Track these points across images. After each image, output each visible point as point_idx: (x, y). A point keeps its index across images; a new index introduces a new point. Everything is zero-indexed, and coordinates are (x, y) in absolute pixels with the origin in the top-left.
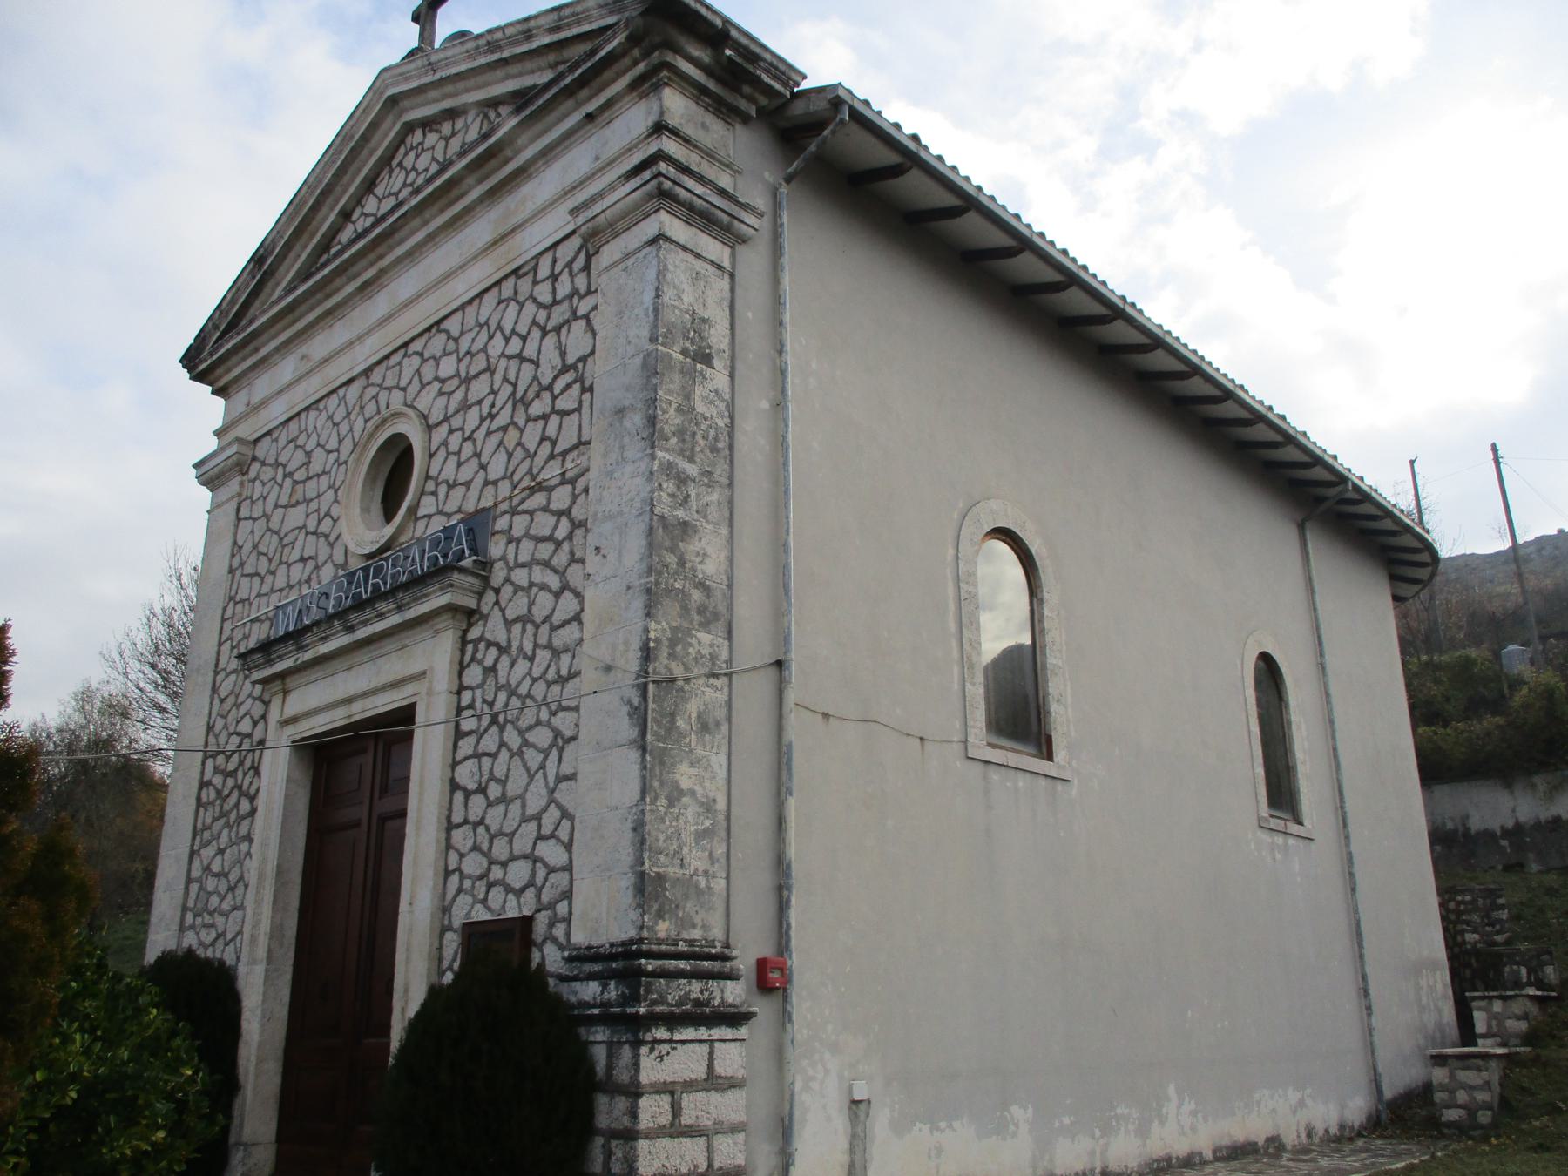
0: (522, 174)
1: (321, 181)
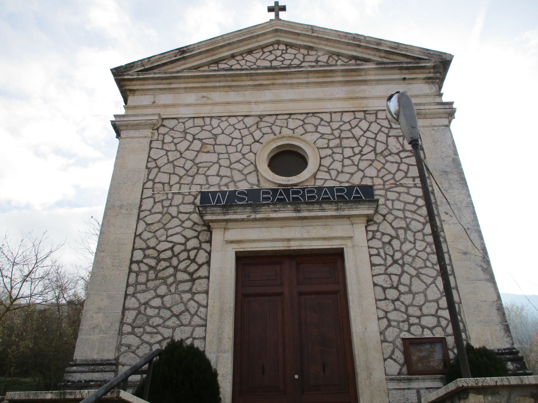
0: (365, 82)
1: (230, 39)
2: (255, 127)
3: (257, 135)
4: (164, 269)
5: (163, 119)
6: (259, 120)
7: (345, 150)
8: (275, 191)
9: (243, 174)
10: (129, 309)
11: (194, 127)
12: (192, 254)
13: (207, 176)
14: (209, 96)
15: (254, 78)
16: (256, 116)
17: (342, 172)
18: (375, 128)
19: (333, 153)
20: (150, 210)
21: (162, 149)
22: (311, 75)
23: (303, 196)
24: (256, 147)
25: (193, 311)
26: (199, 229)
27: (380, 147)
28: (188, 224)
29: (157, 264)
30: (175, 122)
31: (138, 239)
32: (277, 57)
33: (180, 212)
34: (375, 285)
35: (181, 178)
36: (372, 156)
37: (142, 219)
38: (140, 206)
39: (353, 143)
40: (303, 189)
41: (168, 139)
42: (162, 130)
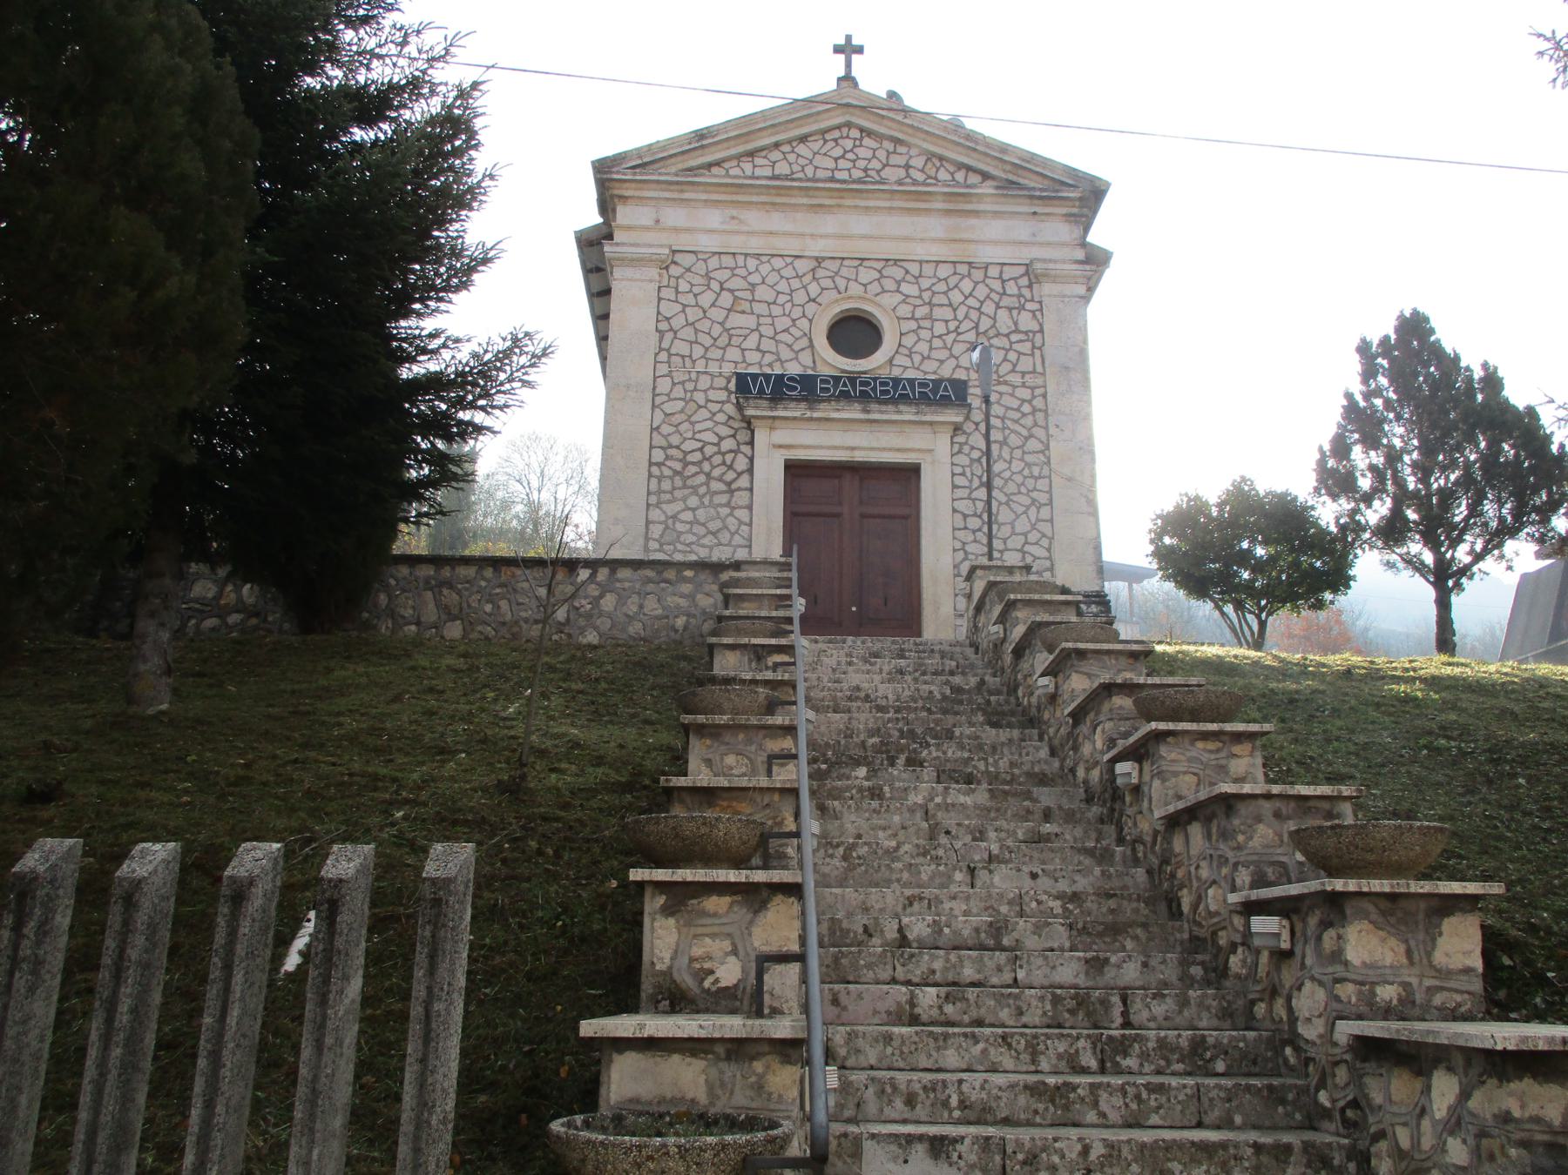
2: (809, 276)
3: (814, 289)
4: (693, 475)
5: (674, 252)
6: (816, 264)
7: (936, 323)
8: (837, 379)
9: (793, 350)
10: (653, 522)
11: (721, 268)
12: (729, 458)
13: (743, 350)
14: (742, 217)
15: (811, 193)
16: (810, 257)
17: (929, 357)
18: (981, 292)
19: (919, 327)
20: (668, 395)
21: (677, 301)
22: (897, 196)
23: (874, 389)
24: (811, 309)
25: (733, 529)
26: (736, 425)
27: (985, 324)
28: (721, 418)
29: (684, 468)
30: (692, 258)
31: (655, 434)
32: (845, 152)
33: (708, 401)
34: (954, 511)
35: (707, 349)
36: (971, 336)
37: (658, 407)
38: (654, 388)
39: (948, 314)
40: (875, 379)
41: (684, 286)
42: (674, 271)
